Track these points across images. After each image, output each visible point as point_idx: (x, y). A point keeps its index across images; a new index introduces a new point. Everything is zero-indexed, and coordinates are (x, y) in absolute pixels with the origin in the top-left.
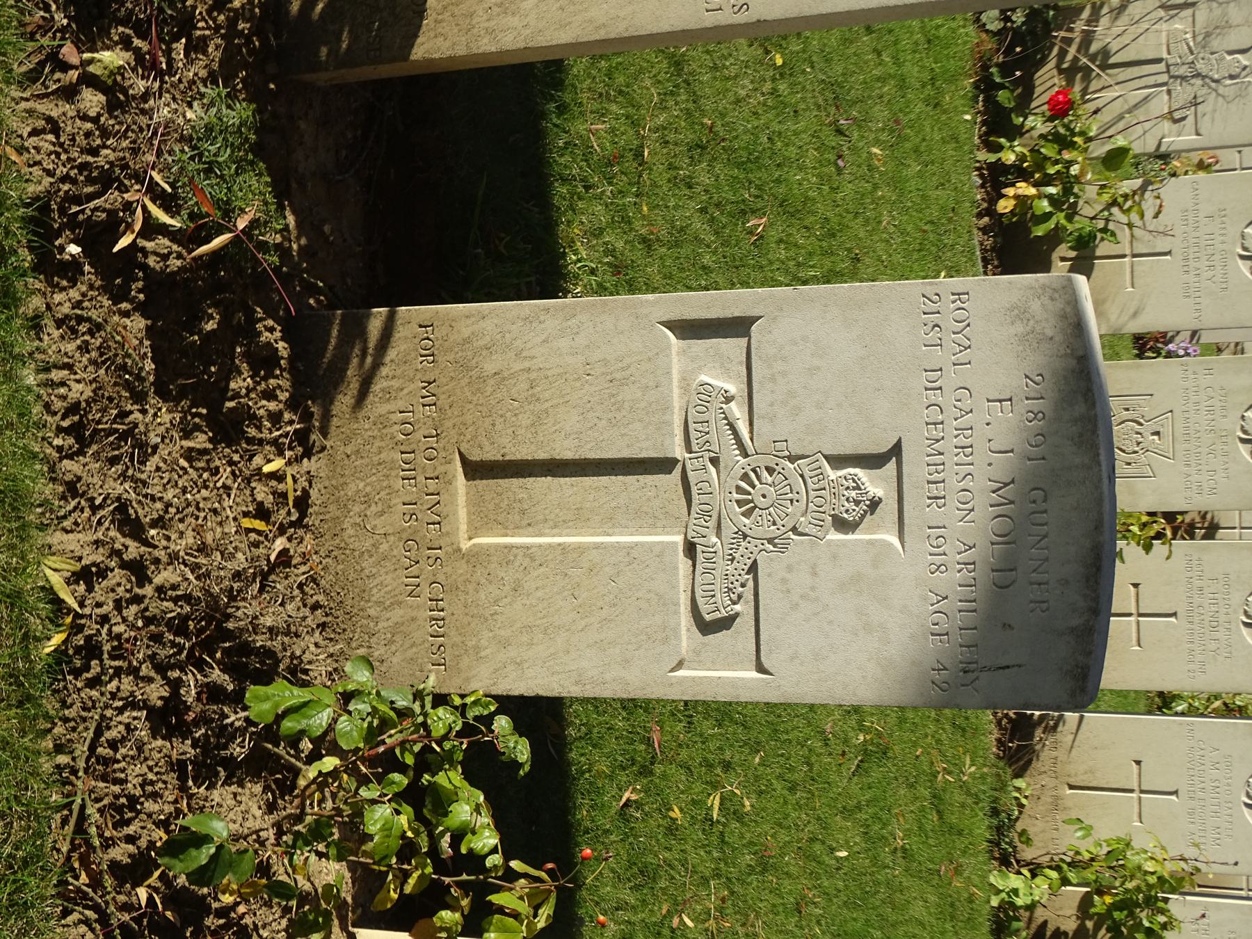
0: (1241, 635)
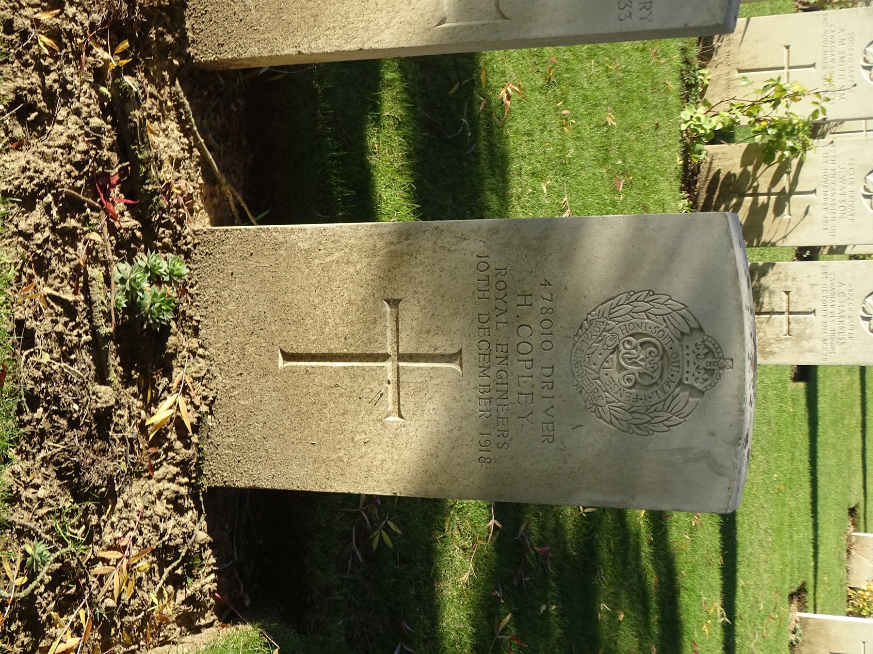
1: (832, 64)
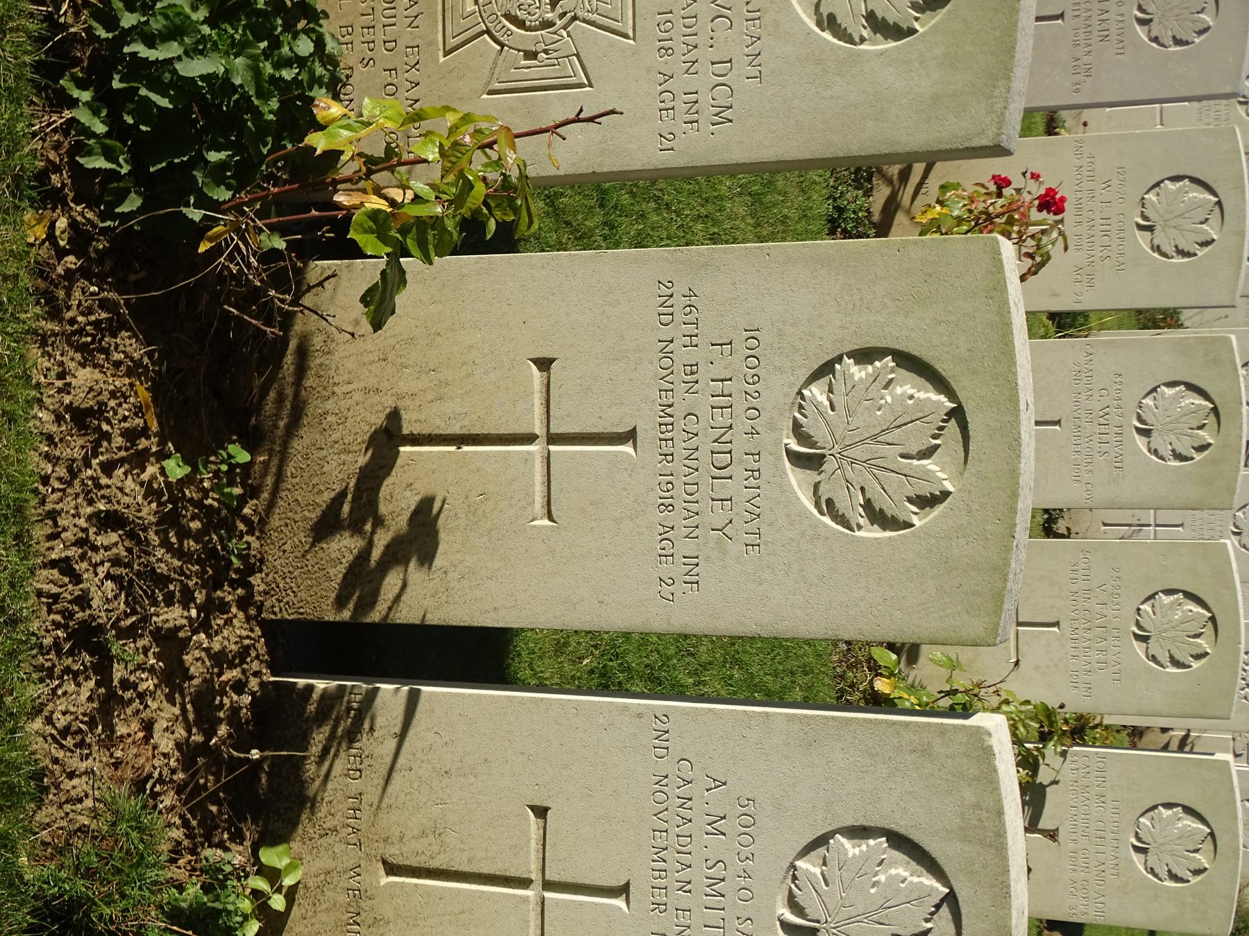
0: (785, 488)
1: (683, 899)
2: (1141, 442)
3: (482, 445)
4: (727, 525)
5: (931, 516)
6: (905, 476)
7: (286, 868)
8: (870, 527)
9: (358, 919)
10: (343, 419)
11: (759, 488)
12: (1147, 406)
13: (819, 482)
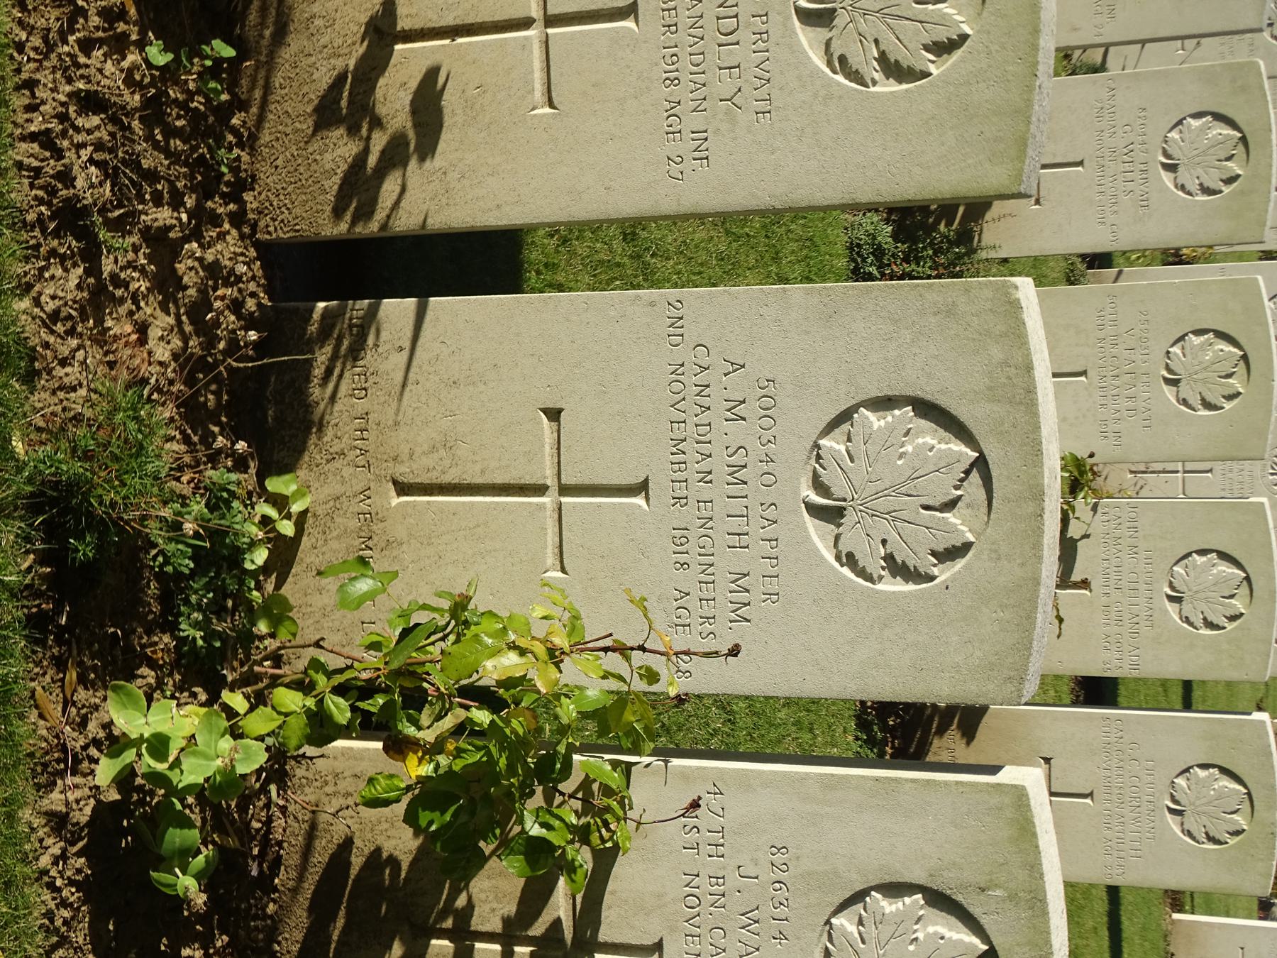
0: (795, 48)
1: (705, 491)
2: (1167, 178)
3: (477, 35)
4: (736, 94)
5: (950, 63)
6: (921, 22)
7: (294, 494)
8: (886, 82)
9: (370, 543)
10: (331, 22)
11: (767, 51)
12: (1174, 140)
13: (831, 39)
